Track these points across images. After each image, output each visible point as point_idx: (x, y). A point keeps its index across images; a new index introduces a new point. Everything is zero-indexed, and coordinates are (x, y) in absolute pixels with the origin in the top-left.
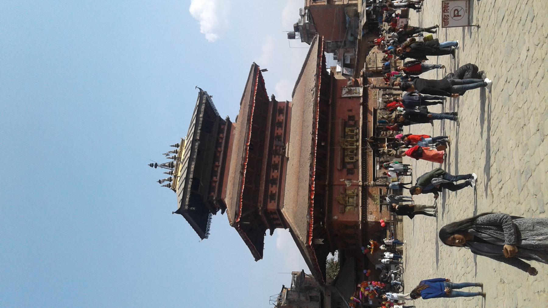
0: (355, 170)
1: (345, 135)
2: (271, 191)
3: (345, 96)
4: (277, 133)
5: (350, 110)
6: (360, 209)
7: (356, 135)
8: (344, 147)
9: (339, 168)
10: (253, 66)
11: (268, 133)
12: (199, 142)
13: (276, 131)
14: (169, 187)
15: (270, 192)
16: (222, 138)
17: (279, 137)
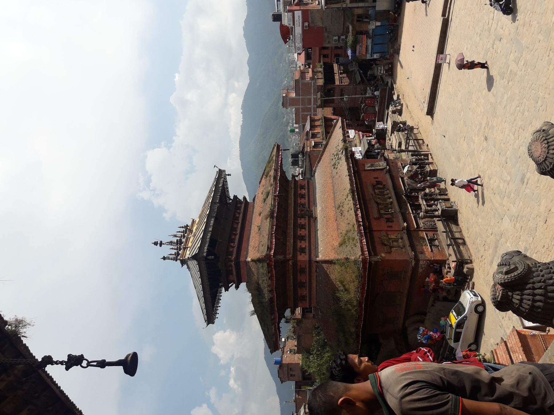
0: (394, 219)
9: (376, 215)
14: (176, 261)
15: (299, 247)
16: (239, 214)
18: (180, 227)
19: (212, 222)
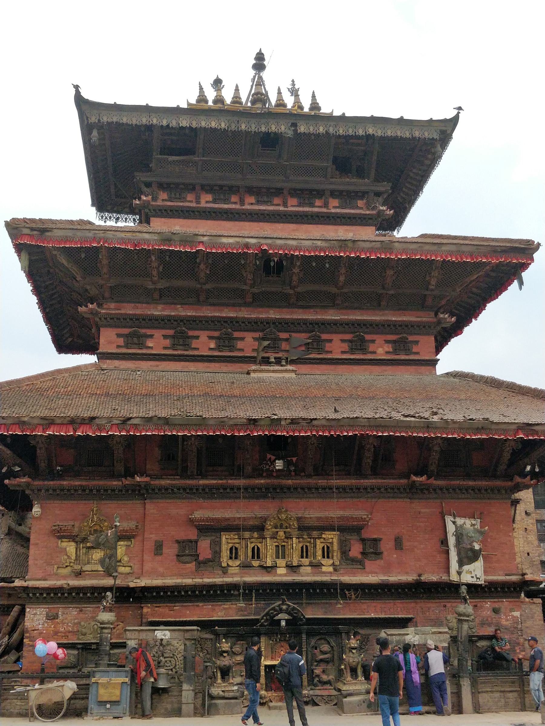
1: (305, 528)
2: (151, 336)
3: (451, 528)
4: (330, 341)
5: (398, 543)
6: (59, 583)
7: (311, 565)
8: (269, 525)
10: (529, 242)
11: (332, 315)
12: (290, 133)
13: (336, 338)
14: (198, 101)
15: (149, 332)
17: (317, 344)
18: (314, 96)
19: (213, 125)
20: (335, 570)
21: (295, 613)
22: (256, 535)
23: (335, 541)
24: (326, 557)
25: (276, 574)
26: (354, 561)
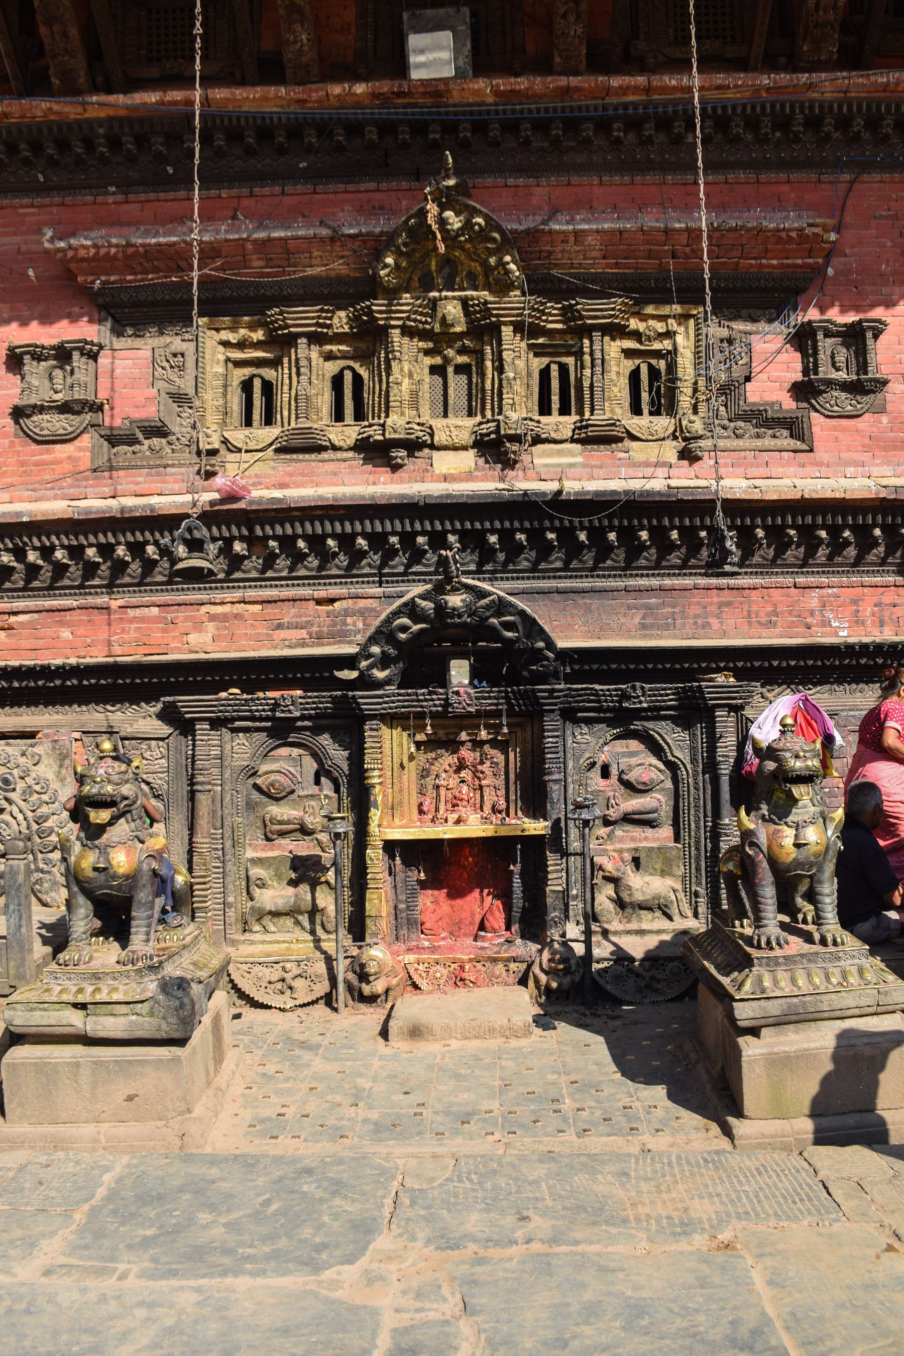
20: (688, 456)
21: (509, 626)
22: (340, 321)
23: (684, 342)
24: (646, 411)
25: (426, 474)
26: (764, 420)
